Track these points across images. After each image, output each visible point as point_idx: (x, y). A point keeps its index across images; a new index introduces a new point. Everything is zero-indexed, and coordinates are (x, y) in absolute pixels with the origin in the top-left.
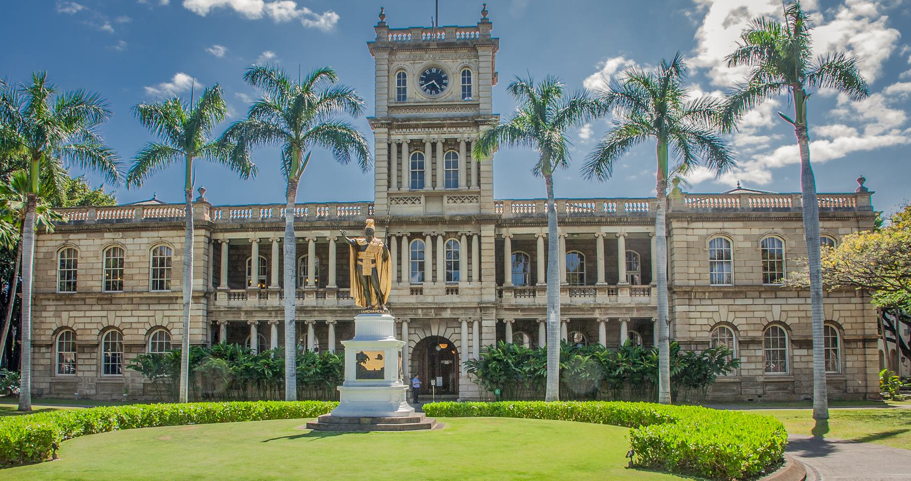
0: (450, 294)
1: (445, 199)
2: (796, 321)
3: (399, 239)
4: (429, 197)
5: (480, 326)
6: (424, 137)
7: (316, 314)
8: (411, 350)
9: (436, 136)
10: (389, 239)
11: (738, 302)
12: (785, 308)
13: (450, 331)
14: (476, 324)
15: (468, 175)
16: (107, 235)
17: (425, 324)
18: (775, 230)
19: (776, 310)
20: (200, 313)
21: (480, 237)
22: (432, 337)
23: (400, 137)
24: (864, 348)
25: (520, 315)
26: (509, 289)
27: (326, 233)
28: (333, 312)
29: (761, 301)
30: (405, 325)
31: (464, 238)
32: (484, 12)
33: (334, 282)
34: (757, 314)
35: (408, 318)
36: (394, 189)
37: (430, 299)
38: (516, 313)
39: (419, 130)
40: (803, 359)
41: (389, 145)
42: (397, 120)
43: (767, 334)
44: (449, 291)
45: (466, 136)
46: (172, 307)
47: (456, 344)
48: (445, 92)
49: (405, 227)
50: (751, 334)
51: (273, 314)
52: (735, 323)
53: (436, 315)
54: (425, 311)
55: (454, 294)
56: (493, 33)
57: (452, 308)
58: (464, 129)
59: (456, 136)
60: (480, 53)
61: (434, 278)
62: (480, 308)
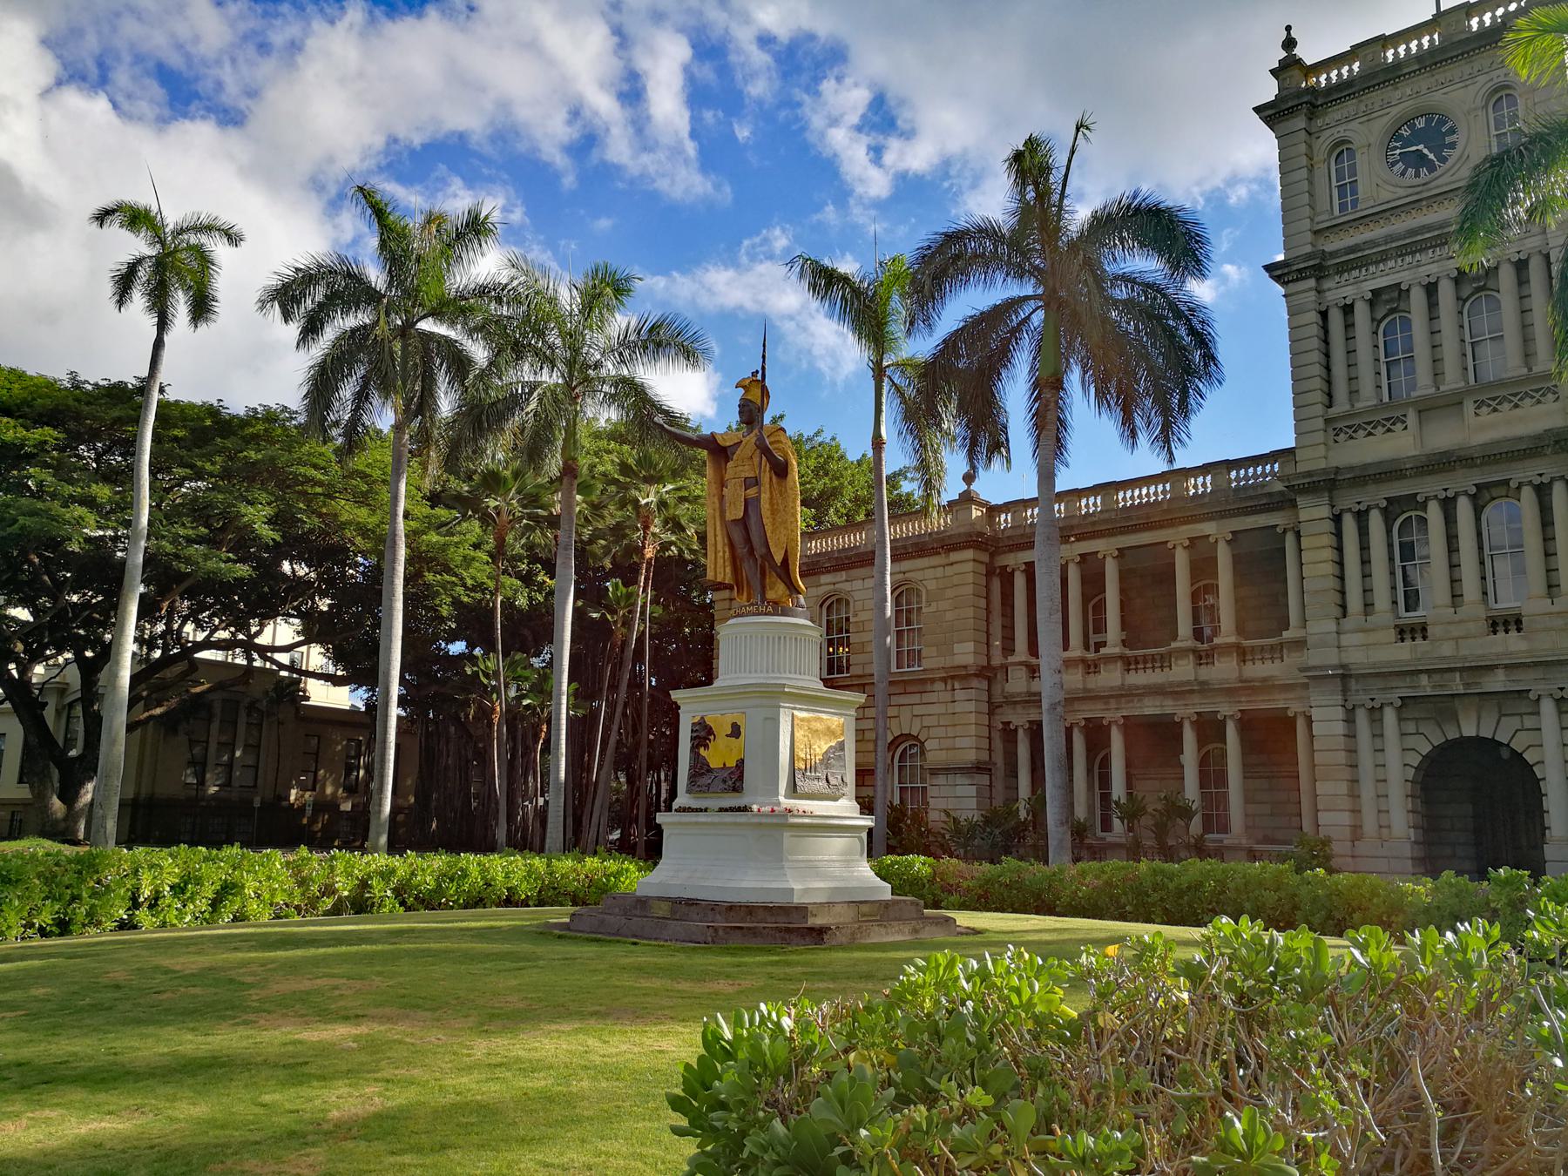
1: (1469, 407)
3: (1361, 517)
6: (1404, 277)
7: (1196, 699)
8: (1411, 773)
9: (1433, 269)
10: (1337, 519)
13: (1514, 722)
15: (1527, 340)
16: (825, 579)
17: (1442, 707)
20: (971, 706)
22: (1463, 742)
23: (1349, 292)
27: (1209, 528)
28: (1230, 692)
30: (1390, 716)
31: (1527, 493)
33: (1233, 627)
35: (1394, 696)
36: (1342, 406)
37: (1447, 649)
39: (1391, 264)
41: (1324, 315)
42: (1333, 254)
46: (927, 698)
47: (1529, 757)
49: (1371, 488)
53: (1467, 685)
54: (1436, 677)
55: (1513, 633)
57: (1507, 667)
61: (1456, 597)
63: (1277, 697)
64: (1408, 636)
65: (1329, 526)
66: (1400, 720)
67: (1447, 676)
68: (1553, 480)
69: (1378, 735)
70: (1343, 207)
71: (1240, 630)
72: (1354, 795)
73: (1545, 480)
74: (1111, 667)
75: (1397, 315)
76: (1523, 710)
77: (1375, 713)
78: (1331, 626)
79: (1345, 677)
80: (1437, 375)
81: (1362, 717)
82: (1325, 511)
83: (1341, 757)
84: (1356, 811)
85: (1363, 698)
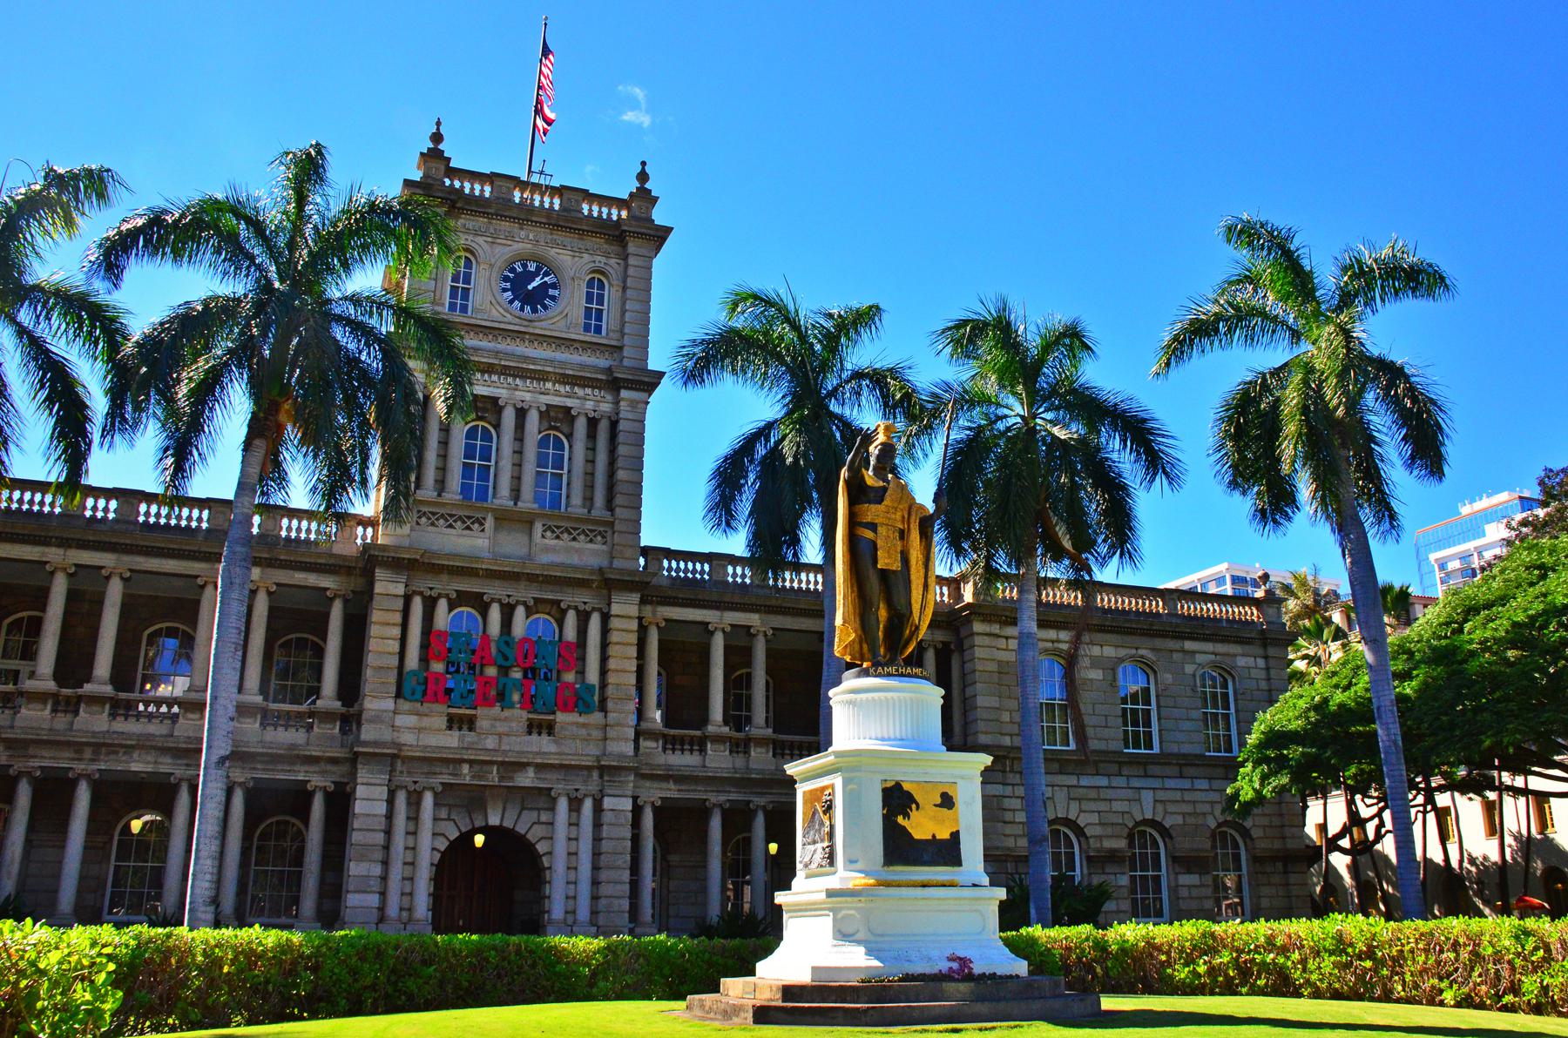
0: (534, 737)
1: (538, 528)
2: (1180, 820)
3: (430, 605)
4: (505, 519)
5: (598, 809)
9: (528, 396)
10: (408, 599)
11: (1085, 781)
12: (1161, 795)
13: (529, 817)
14: (588, 805)
15: (589, 487)
17: (471, 799)
18: (1141, 652)
19: (1148, 797)
21: (606, 618)
24: (1286, 872)
25: (672, 791)
26: (653, 735)
29: (1121, 781)
30: (428, 799)
32: (643, 177)
34: (1117, 806)
35: (436, 781)
36: (427, 492)
37: (490, 743)
38: (664, 785)
39: (495, 378)
40: (1195, 893)
43: (1131, 845)
44: (533, 727)
45: (589, 405)
47: (541, 848)
48: (550, 313)
49: (445, 577)
50: (1107, 844)
51: (88, 753)
52: (1081, 822)
53: (501, 779)
54: (476, 768)
55: (545, 738)
56: (659, 216)
57: (540, 767)
58: (589, 391)
59: (569, 402)
60: (631, 248)
62: (603, 770)
63: (297, 768)
64: (455, 726)
65: (400, 603)
66: (436, 804)
67: (485, 768)
68: (594, 609)
69: (414, 817)
70: (452, 307)
71: (263, 690)
72: (384, 878)
73: (588, 608)
74: (95, 708)
75: (481, 423)
76: (541, 805)
77: (415, 801)
78: (389, 704)
79: (391, 758)
80: (516, 494)
81: (401, 797)
82: (400, 589)
83: (380, 838)
84: (383, 894)
85: (407, 779)
